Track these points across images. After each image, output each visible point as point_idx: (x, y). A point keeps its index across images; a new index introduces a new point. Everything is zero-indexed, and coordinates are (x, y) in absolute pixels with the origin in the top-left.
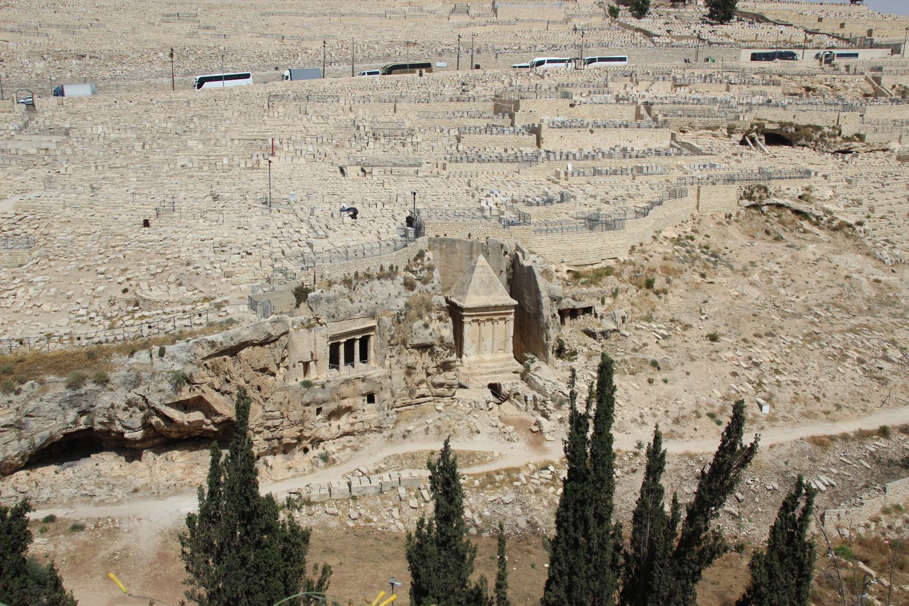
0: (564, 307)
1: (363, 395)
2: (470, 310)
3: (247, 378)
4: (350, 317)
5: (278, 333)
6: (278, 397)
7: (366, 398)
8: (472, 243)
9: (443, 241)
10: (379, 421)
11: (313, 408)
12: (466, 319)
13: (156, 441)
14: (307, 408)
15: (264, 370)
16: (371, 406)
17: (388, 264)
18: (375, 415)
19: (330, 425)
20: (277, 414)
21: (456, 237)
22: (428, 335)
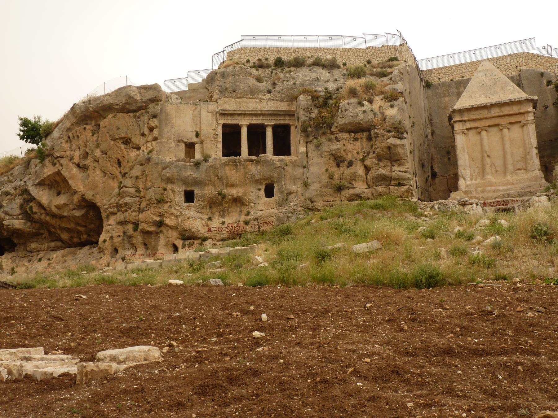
1: (257, 182)
3: (103, 146)
4: (252, 93)
6: (136, 171)
7: (263, 187)
11: (180, 190)
13: (53, 244)
14: (169, 186)
16: (268, 199)
18: (275, 211)
19: (210, 219)
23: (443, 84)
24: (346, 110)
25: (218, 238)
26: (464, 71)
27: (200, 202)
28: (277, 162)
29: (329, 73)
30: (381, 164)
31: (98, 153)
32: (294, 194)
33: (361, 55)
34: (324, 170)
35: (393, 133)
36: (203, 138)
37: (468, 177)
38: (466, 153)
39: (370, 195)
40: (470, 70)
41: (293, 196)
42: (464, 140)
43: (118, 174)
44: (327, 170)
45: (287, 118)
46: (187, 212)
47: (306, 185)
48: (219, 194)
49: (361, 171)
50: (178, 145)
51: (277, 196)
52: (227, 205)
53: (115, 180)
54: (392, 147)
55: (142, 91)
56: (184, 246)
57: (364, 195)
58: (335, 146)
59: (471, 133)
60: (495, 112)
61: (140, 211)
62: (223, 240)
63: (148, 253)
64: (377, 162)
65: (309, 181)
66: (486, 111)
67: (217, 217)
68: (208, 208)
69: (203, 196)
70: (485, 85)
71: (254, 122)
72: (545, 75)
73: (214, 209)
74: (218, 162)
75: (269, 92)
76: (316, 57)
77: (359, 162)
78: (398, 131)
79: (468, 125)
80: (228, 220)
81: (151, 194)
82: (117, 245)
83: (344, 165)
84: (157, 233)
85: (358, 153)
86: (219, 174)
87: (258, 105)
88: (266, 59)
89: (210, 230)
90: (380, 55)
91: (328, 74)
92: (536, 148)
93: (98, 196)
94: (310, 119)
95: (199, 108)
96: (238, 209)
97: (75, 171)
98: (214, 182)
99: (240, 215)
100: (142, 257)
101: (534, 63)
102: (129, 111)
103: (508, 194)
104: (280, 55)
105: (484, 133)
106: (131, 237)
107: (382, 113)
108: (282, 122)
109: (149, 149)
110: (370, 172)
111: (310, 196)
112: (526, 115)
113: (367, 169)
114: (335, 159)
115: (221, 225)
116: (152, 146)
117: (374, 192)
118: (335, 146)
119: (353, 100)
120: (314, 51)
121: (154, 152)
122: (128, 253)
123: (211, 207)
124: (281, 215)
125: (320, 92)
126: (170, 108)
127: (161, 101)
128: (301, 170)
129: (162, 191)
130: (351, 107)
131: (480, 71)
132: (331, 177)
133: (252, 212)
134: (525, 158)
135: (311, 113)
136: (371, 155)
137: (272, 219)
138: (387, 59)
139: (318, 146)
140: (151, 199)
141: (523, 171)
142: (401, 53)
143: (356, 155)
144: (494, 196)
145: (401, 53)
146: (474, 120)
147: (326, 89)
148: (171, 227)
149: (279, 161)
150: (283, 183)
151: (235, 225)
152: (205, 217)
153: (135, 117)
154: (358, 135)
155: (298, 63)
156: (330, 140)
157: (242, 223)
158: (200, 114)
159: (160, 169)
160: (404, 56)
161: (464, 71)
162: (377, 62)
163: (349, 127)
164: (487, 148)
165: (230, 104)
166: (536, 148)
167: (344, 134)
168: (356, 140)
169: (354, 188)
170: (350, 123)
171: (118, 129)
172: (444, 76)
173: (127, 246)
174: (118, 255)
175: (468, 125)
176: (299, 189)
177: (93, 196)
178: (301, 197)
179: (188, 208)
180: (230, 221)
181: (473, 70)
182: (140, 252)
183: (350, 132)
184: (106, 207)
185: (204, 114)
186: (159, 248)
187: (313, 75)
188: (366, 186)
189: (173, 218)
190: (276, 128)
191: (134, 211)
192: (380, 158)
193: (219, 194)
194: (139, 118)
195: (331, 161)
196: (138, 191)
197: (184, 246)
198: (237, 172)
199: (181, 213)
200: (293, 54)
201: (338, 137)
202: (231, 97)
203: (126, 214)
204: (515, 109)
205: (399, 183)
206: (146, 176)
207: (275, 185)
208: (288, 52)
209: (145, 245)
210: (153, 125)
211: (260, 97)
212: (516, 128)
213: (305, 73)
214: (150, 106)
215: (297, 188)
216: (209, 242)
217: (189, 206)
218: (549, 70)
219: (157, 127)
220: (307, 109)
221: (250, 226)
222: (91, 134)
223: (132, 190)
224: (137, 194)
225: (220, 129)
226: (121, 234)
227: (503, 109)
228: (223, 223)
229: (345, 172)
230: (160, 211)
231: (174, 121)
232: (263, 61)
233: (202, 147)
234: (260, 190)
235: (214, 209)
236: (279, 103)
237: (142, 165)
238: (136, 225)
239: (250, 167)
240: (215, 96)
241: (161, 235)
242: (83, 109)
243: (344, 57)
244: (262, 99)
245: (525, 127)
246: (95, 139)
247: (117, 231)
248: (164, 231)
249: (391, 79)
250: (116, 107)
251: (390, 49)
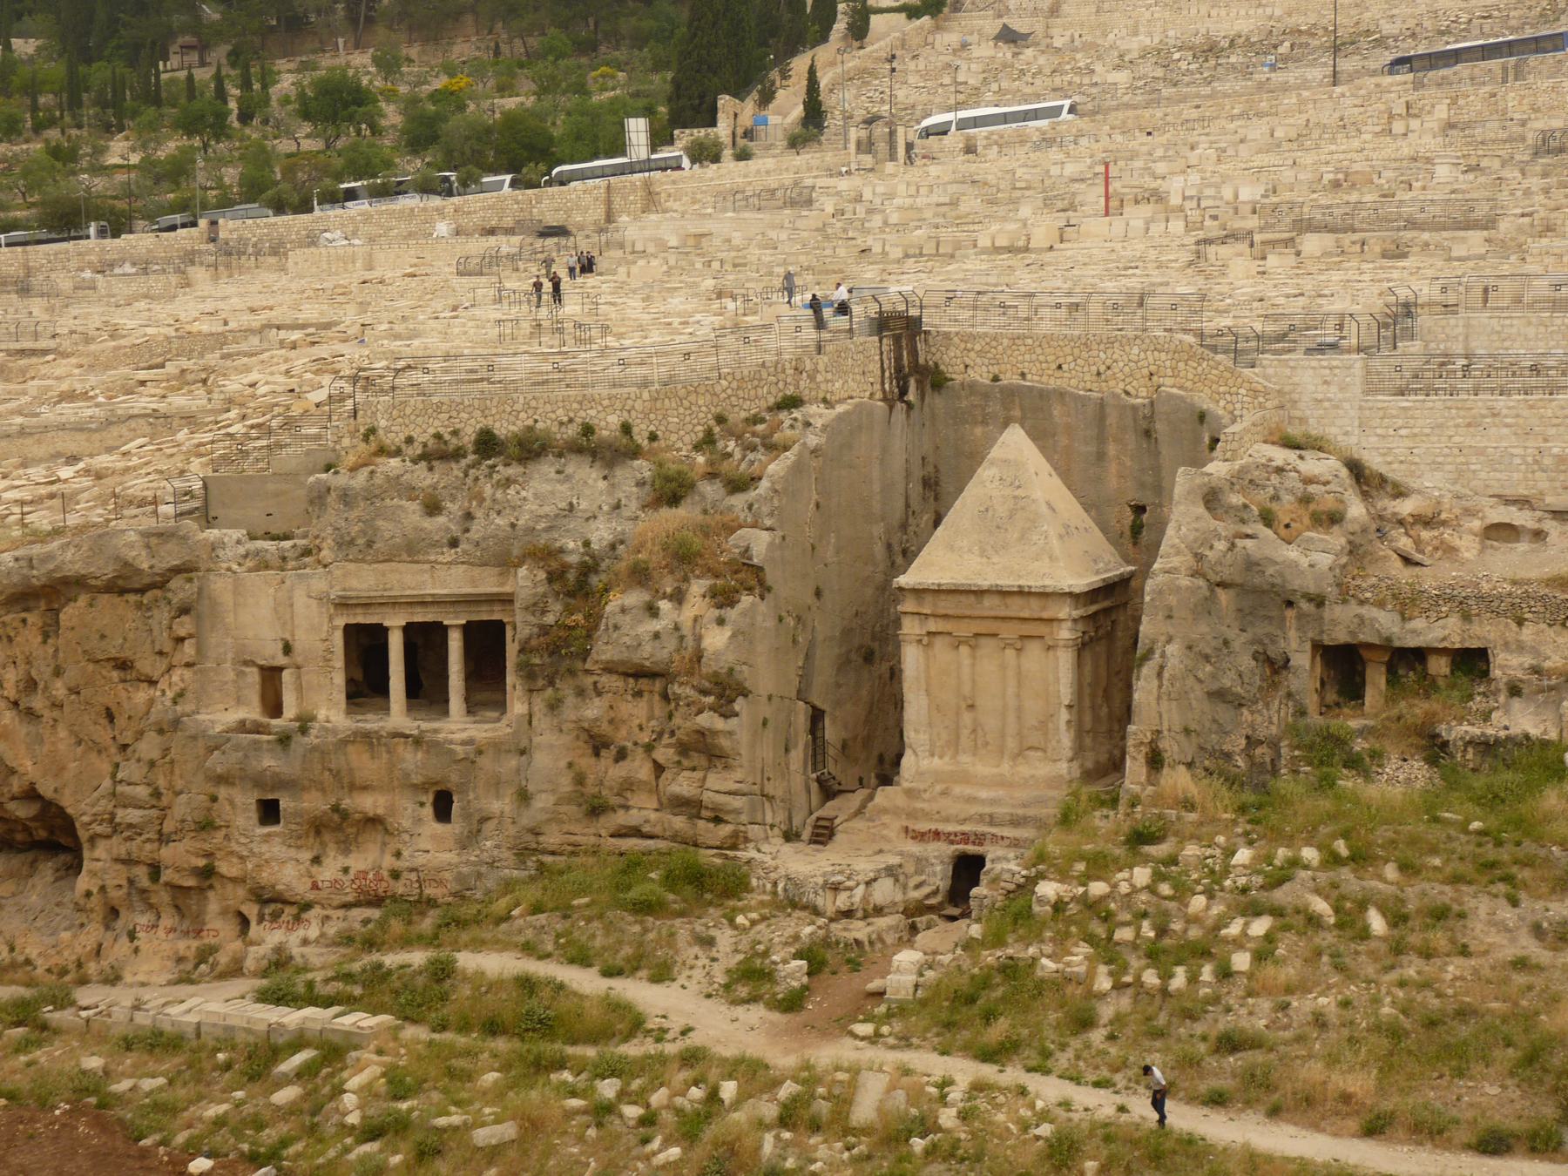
0: (1341, 636)
2: (919, 592)
4: (412, 550)
5: (163, 565)
7: (429, 799)
8: (1102, 404)
9: (1011, 393)
10: (460, 878)
12: (910, 627)
14: (223, 792)
15: (123, 665)
16: (439, 828)
17: (614, 420)
18: (451, 857)
19: (316, 860)
20: (142, 792)
21: (1053, 383)
23: (972, 387)
24: (616, 627)
25: (335, 903)
26: (1027, 357)
27: (293, 827)
28: (459, 748)
29: (605, 478)
30: (686, 763)
31: (59, 689)
32: (495, 821)
33: (701, 402)
34: (563, 764)
35: (711, 699)
36: (299, 660)
38: (923, 692)
39: (658, 830)
40: (1042, 358)
41: (490, 825)
42: (921, 660)
43: (110, 742)
44: (570, 765)
45: (497, 608)
46: (265, 848)
47: (524, 797)
48: (336, 809)
49: (644, 772)
50: (243, 673)
51: (456, 827)
52: (354, 830)
53: (104, 756)
55: (154, 541)
56: (261, 919)
57: (646, 829)
58: (593, 710)
59: (939, 642)
60: (990, 605)
61: (163, 839)
62: (346, 906)
63: (184, 927)
64: (676, 758)
65: (531, 788)
66: (972, 598)
67: (332, 854)
68: (312, 834)
69: (297, 814)
71: (418, 619)
72: (1207, 419)
73: (327, 837)
74: (330, 739)
75: (454, 543)
76: (579, 420)
77: (640, 750)
78: (726, 691)
79: (933, 626)
80: (360, 861)
81: (183, 808)
82: (116, 903)
83: (608, 755)
84: (201, 890)
85: (641, 728)
86: (332, 766)
87: (426, 576)
88: (455, 433)
89: (315, 887)
90: (753, 393)
91: (602, 484)
92: (1069, 707)
93: (67, 792)
94: (545, 630)
95: (288, 582)
96: (379, 838)
97: (9, 717)
98: (321, 783)
99: (383, 852)
100: (171, 936)
101: (1190, 376)
102: (123, 592)
103: (991, 816)
104: (489, 422)
105: (964, 650)
106: (144, 891)
107: (699, 639)
108: (485, 618)
109: (177, 689)
110: (664, 776)
111: (532, 824)
112: (1055, 624)
113: (659, 769)
114: (591, 737)
115: (340, 876)
116: (182, 680)
118: (593, 710)
119: (636, 598)
120: (575, 406)
121: (189, 695)
122: (144, 919)
123: (318, 833)
124: (465, 870)
125: (572, 552)
126: (220, 586)
127: (197, 570)
128: (513, 762)
129: (208, 804)
130: (628, 618)
132: (580, 780)
133: (405, 853)
134: (1043, 725)
135: (544, 612)
136: (666, 740)
137: (447, 875)
138: (771, 401)
139: (554, 706)
140: (183, 821)
141: (1039, 754)
142: (812, 378)
143: (637, 730)
144: (962, 816)
145: (812, 378)
146: (946, 616)
147: (587, 544)
148: (233, 880)
149: (464, 743)
150: (471, 796)
151: (371, 876)
152: (306, 856)
153: (139, 606)
154: (644, 684)
155: (530, 449)
156: (581, 693)
157: (385, 874)
158: (290, 598)
159: (202, 752)
160: (823, 386)
162: (743, 415)
163: (620, 670)
164: (966, 689)
165: (364, 580)
166: (1069, 707)
167: (614, 677)
168: (638, 694)
169: (627, 808)
170: (623, 663)
171: (103, 637)
172: (978, 361)
173: (139, 906)
174: (119, 924)
175: (933, 626)
176: (507, 809)
177: (56, 790)
178: (511, 827)
179: (267, 838)
180: (362, 867)
181: (1051, 358)
182: (167, 921)
183: (627, 675)
184: (85, 819)
185: (300, 599)
186: (208, 918)
187: (564, 493)
188: (655, 805)
189: (235, 860)
190: (471, 631)
191: (148, 840)
192: (684, 749)
193: (336, 809)
194: (149, 609)
195: (581, 743)
196: (157, 794)
197: (261, 919)
198: (373, 758)
199: (251, 850)
200: (523, 415)
201: (600, 686)
202: (363, 561)
203: (133, 846)
204: (1032, 608)
206: (172, 762)
207: (455, 798)
208: (508, 409)
209: (177, 907)
210: (182, 633)
211: (432, 558)
212: (1034, 650)
213: (546, 488)
214: (173, 584)
215: (501, 805)
216: (316, 911)
217: (269, 835)
218: (1222, 403)
219: (191, 636)
220: (535, 604)
221: (402, 881)
222: (40, 639)
223: (142, 792)
224: (154, 802)
225: (338, 639)
226: (124, 883)
227: (1009, 601)
228: (346, 870)
229: (610, 772)
230: (207, 846)
231: (230, 619)
232: (447, 437)
233: (299, 677)
234: (422, 804)
235: (327, 837)
236: (477, 571)
237: (161, 732)
238: (155, 870)
239: (400, 749)
240: (326, 554)
241: (211, 894)
242: (15, 579)
243: (652, 416)
244: (436, 562)
245: (1051, 653)
246: (51, 651)
247: (115, 877)
248: (217, 885)
249: (750, 507)
250: (93, 582)
251: (784, 371)
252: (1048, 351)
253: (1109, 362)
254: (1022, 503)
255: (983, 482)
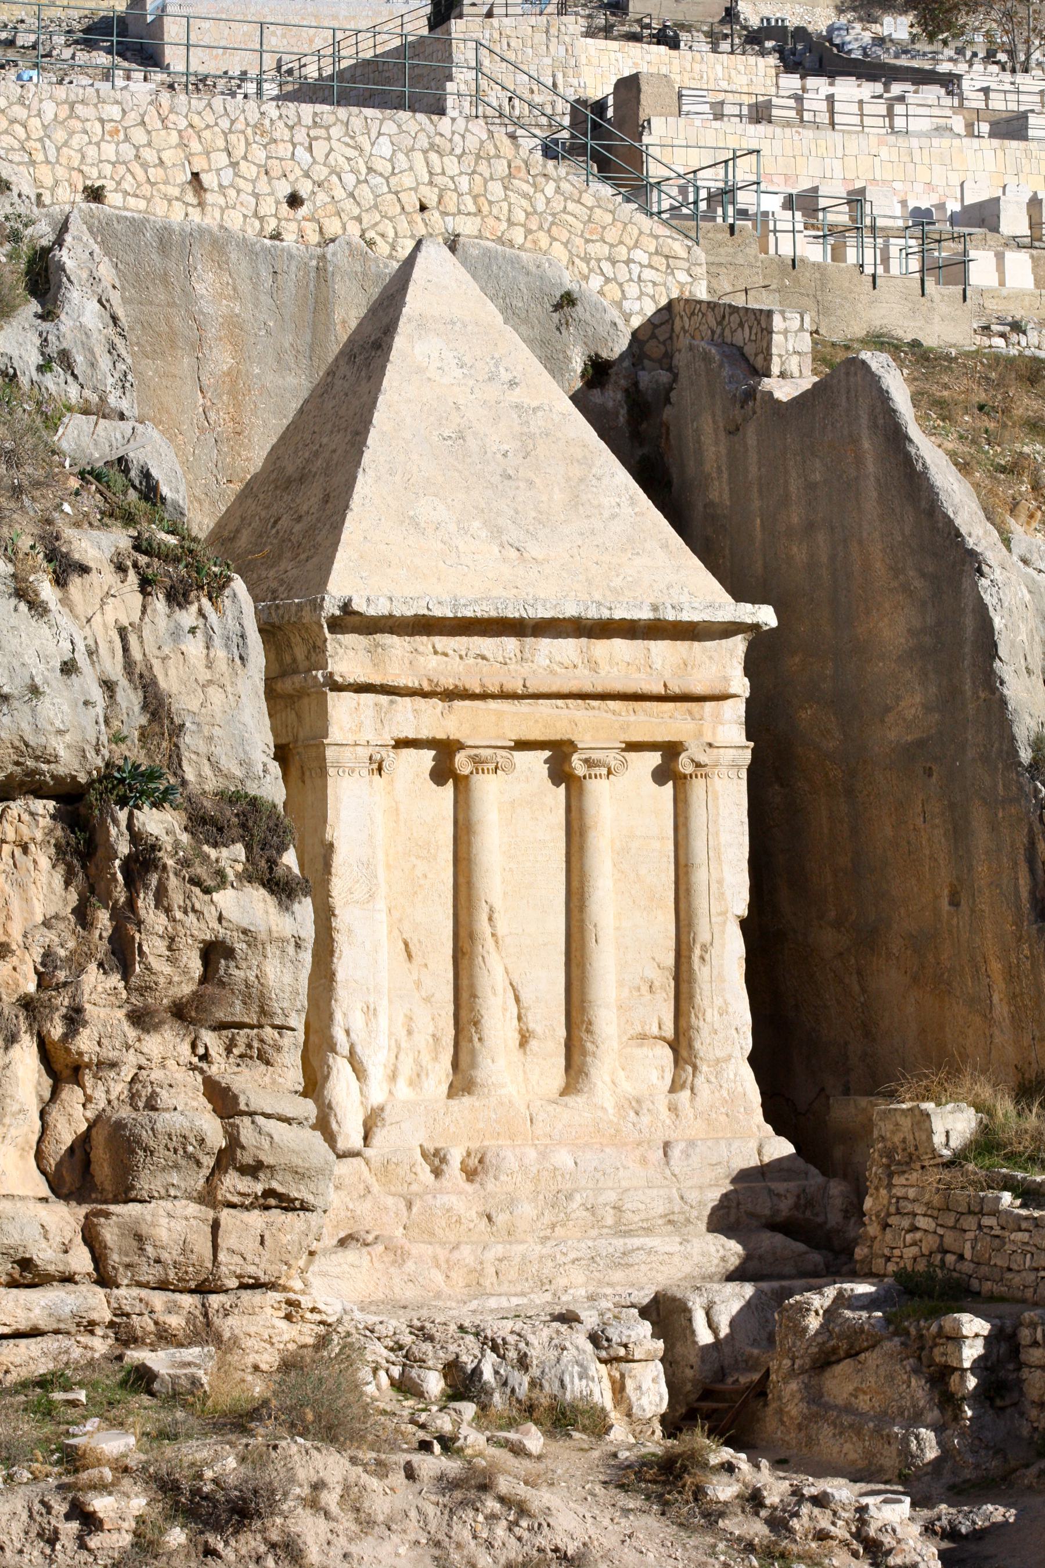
22: (45, 673)
26: (109, 151)
37: (376, 1064)
38: (381, 905)
54: (240, 946)
60: (556, 659)
70: (472, 444)
101: (520, 216)
117: (109, 1233)
131: (421, 324)
161: (109, 151)
205: (269, 1193)
218: (596, 282)
252: (161, 138)
253: (320, 172)
254: (537, 423)
255: (420, 370)
